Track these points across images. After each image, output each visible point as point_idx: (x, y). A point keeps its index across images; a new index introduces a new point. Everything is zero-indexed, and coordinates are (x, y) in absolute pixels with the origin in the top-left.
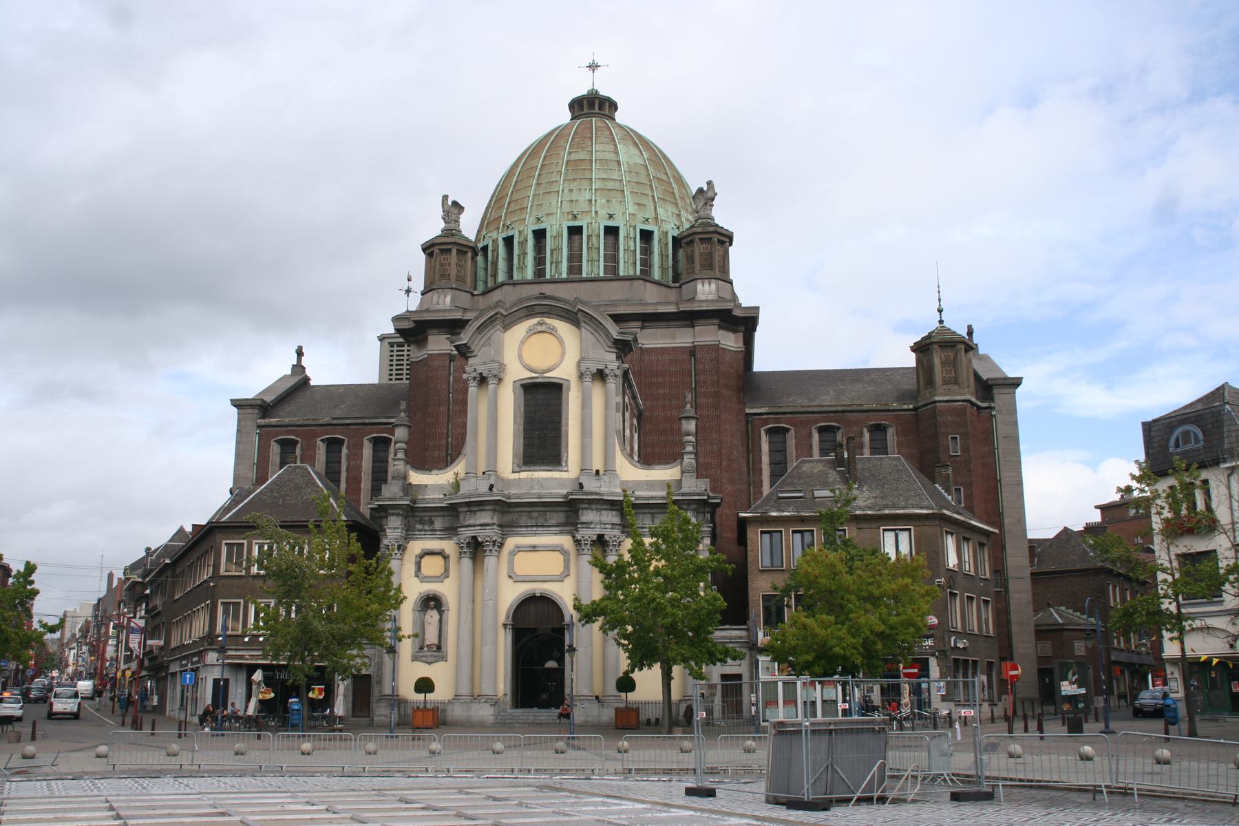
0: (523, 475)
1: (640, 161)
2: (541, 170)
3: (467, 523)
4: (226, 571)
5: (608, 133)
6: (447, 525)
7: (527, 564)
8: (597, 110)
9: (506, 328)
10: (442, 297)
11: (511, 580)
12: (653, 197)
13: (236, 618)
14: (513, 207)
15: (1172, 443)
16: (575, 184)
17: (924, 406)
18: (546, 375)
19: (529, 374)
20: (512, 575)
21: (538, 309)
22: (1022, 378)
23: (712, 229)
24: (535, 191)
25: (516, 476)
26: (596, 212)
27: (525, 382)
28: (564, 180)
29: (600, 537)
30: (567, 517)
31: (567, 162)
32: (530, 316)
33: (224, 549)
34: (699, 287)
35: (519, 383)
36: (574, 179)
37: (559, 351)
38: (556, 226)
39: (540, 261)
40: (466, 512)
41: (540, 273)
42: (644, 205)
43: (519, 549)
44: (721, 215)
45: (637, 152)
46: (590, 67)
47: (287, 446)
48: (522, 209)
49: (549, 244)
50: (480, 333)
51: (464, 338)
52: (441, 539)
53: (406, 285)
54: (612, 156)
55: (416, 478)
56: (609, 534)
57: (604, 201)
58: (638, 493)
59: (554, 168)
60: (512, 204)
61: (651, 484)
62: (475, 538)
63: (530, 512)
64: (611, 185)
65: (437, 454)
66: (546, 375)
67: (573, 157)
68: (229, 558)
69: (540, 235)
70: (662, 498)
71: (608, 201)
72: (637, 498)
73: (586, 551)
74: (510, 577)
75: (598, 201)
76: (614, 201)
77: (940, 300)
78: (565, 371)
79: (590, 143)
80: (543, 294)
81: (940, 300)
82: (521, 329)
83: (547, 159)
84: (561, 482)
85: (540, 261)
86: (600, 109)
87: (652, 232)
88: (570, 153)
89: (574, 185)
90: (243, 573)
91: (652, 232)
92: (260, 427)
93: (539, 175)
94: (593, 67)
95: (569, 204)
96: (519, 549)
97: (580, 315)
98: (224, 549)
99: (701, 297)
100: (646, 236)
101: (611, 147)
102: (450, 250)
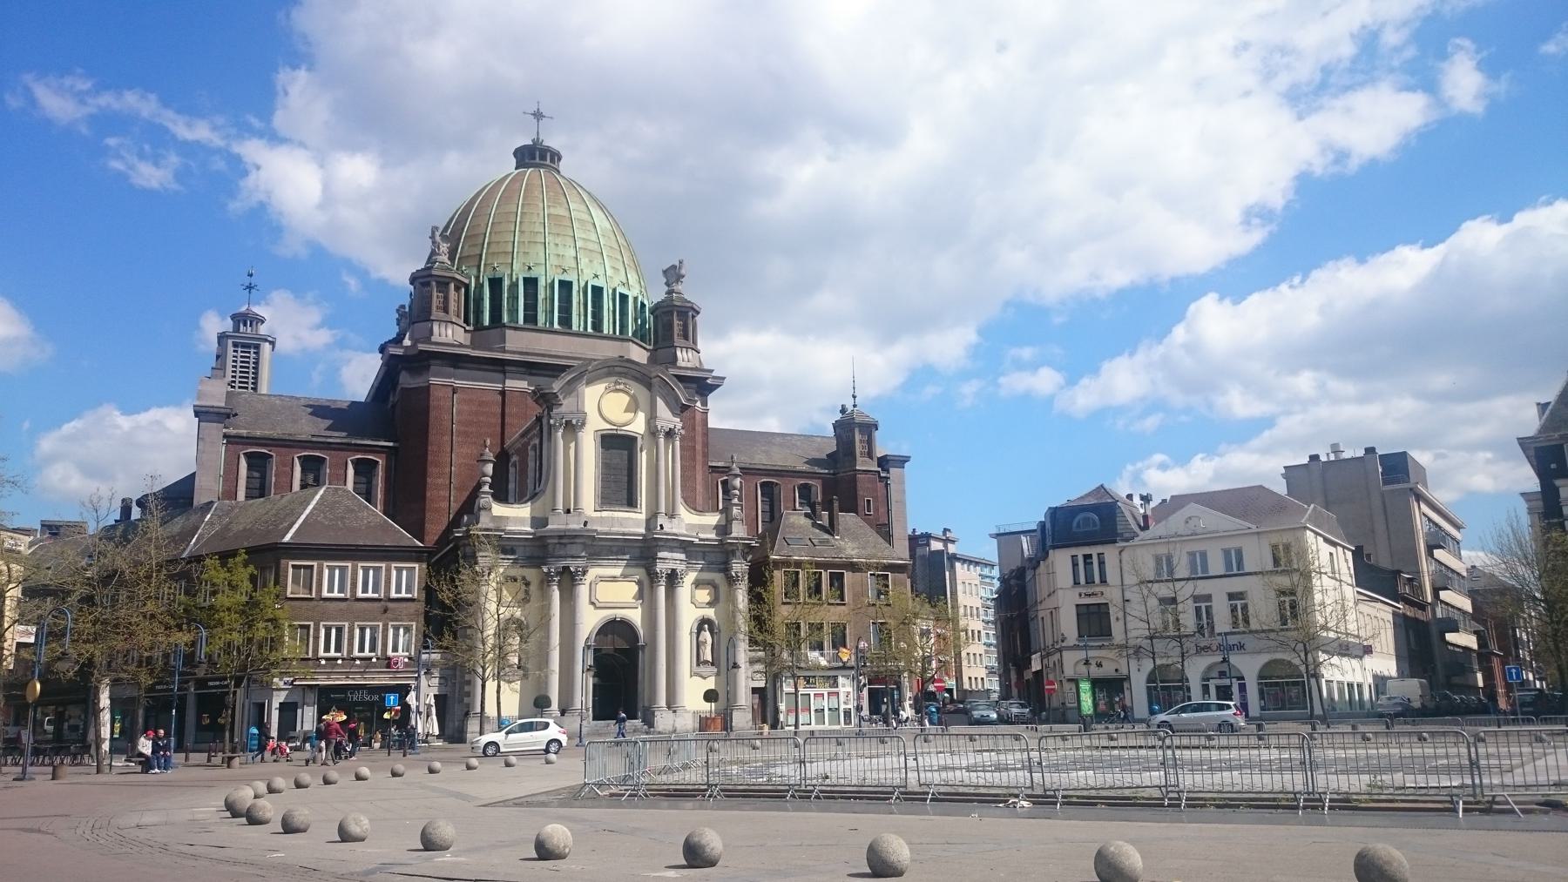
0: (605, 514)
1: (609, 226)
2: (521, 218)
3: (557, 553)
4: (292, 593)
5: (575, 192)
6: (527, 554)
7: (606, 592)
8: (548, 162)
9: (589, 383)
10: (443, 329)
11: (592, 607)
12: (624, 262)
13: (305, 640)
14: (494, 248)
15: (1075, 524)
16: (560, 239)
17: (843, 472)
18: (623, 428)
19: (609, 427)
20: (596, 602)
21: (617, 369)
22: (910, 457)
23: (689, 305)
24: (519, 237)
25: (598, 514)
26: (582, 270)
27: (605, 432)
28: (549, 233)
29: (674, 571)
30: (642, 552)
31: (548, 215)
32: (609, 374)
33: (290, 570)
34: (679, 353)
35: (600, 433)
36: (558, 234)
37: (603, 402)
38: (547, 275)
39: (531, 307)
40: (556, 544)
41: (531, 317)
42: (618, 270)
43: (603, 579)
44: (689, 291)
45: (604, 216)
46: (534, 114)
47: (258, 463)
48: (506, 253)
49: (541, 295)
50: (569, 385)
51: (556, 386)
52: (522, 567)
53: (247, 281)
54: (586, 217)
55: (498, 510)
56: (680, 567)
57: (587, 260)
58: (702, 536)
59: (535, 219)
60: (493, 246)
61: (703, 528)
62: (566, 568)
63: (611, 546)
64: (591, 246)
65: (440, 481)
66: (623, 428)
67: (553, 211)
68: (296, 581)
69: (531, 283)
70: (716, 540)
71: (591, 261)
72: (701, 540)
73: (661, 583)
74: (593, 603)
75: (582, 260)
76: (595, 262)
77: (854, 388)
78: (638, 426)
79: (565, 200)
80: (623, 357)
81: (854, 388)
82: (600, 388)
83: (526, 207)
84: (636, 523)
85: (531, 307)
86: (541, 159)
87: (628, 296)
88: (549, 207)
89: (558, 240)
90: (314, 596)
91: (628, 296)
92: (225, 436)
93: (521, 223)
94: (538, 115)
95: (556, 257)
96: (603, 579)
97: (654, 380)
98: (290, 570)
99: (680, 363)
100: (624, 298)
101: (583, 208)
102: (447, 284)
